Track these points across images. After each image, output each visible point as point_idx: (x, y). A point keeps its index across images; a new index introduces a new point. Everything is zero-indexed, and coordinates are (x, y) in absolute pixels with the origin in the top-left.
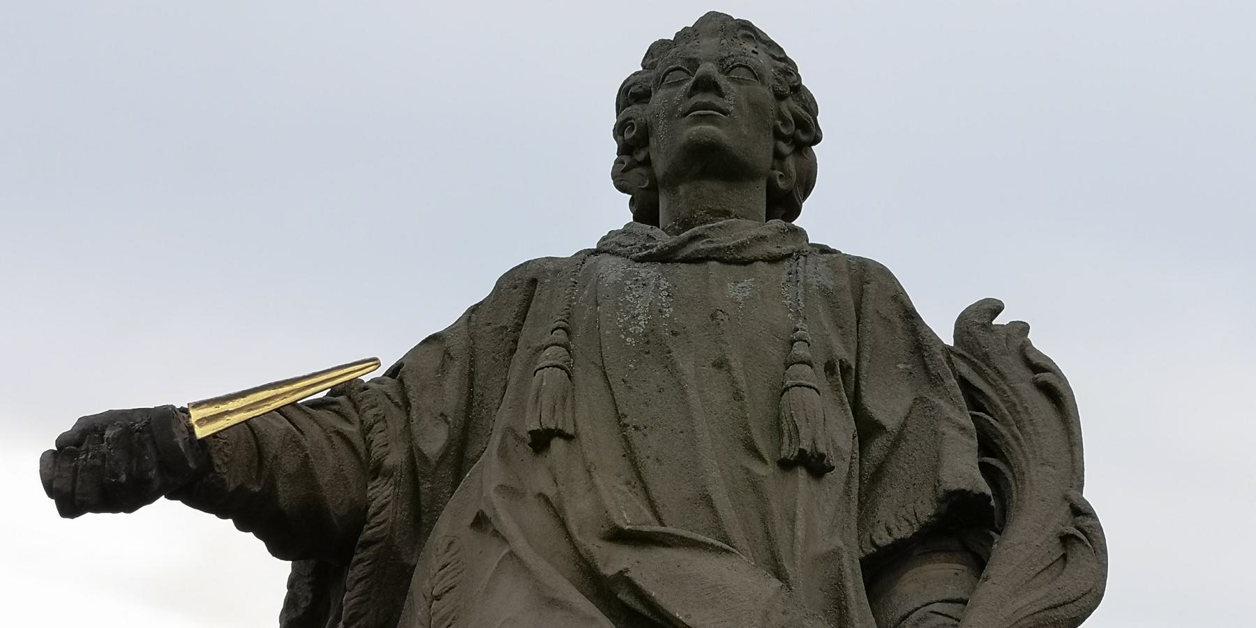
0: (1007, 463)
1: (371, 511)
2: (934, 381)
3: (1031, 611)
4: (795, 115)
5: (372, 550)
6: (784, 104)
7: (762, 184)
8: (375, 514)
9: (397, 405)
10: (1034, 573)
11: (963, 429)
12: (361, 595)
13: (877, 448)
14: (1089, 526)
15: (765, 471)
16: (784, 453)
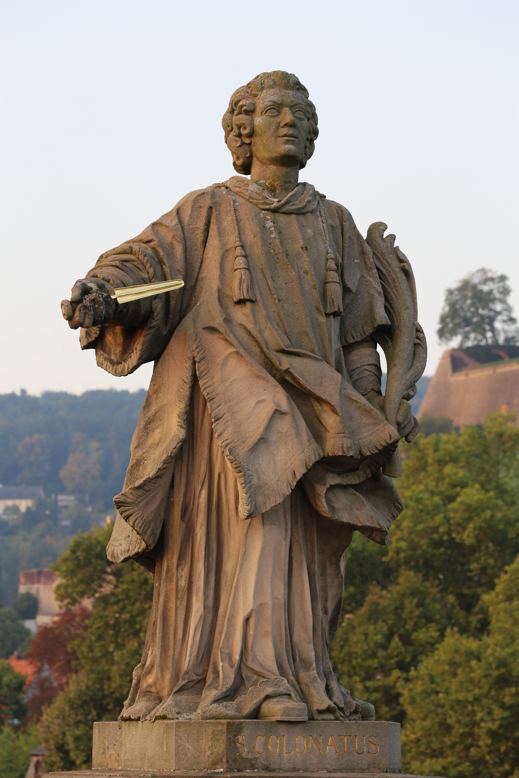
1: (156, 314)
2: (369, 270)
5: (153, 330)
9: (157, 262)
11: (379, 293)
14: (422, 337)
15: (322, 319)
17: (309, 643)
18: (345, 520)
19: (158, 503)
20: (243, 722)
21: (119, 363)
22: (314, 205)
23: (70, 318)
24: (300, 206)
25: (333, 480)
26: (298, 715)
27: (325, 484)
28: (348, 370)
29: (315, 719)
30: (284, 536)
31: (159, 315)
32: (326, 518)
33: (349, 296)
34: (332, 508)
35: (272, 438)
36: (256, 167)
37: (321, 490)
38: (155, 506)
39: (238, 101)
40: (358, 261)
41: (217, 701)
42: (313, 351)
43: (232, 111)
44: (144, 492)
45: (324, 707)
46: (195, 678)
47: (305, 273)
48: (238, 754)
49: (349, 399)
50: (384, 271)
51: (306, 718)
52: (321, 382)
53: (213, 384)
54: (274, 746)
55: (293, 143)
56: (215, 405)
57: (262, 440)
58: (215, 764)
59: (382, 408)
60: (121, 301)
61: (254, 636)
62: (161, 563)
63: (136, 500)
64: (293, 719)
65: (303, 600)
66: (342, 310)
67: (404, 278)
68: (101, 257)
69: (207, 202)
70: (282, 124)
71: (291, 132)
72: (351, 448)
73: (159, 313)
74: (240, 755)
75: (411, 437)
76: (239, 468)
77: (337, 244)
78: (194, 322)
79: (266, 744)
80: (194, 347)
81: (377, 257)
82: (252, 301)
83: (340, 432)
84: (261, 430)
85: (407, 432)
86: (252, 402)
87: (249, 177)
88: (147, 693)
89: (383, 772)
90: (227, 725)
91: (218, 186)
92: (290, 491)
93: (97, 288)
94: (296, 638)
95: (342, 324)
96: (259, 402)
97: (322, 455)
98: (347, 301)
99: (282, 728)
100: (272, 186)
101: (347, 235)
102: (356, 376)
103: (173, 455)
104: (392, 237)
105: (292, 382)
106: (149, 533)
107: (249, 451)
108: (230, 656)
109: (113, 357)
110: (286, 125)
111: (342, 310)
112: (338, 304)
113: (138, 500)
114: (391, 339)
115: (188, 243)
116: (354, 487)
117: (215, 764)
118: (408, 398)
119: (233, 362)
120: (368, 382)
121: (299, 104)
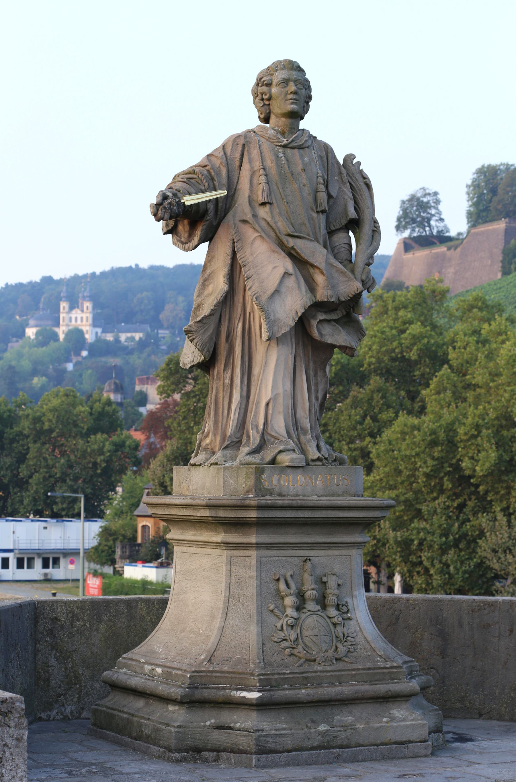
5: (208, 222)
11: (351, 198)
15: (315, 215)
17: (306, 418)
18: (329, 342)
21: (186, 243)
22: (309, 143)
23: (155, 215)
24: (301, 143)
25: (322, 316)
26: (299, 463)
27: (316, 319)
28: (331, 247)
32: (317, 340)
33: (332, 201)
34: (321, 334)
35: (283, 290)
36: (273, 119)
37: (314, 323)
38: (209, 333)
39: (262, 78)
41: (249, 454)
42: (309, 235)
43: (257, 84)
45: (315, 457)
46: (235, 440)
49: (332, 265)
50: (354, 184)
51: (305, 464)
54: (284, 481)
56: (247, 269)
57: (277, 291)
58: (248, 492)
59: (353, 271)
60: (187, 204)
61: (272, 414)
62: (214, 369)
64: (296, 464)
65: (302, 391)
66: (327, 209)
67: (366, 189)
68: (175, 176)
69: (242, 141)
70: (289, 92)
75: (370, 289)
76: (262, 309)
77: (324, 167)
78: (234, 216)
79: (279, 480)
80: (234, 232)
81: (349, 176)
84: (276, 285)
85: (368, 286)
86: (270, 267)
87: (268, 125)
88: (206, 449)
91: (249, 131)
94: (298, 415)
95: (327, 218)
96: (274, 267)
97: (314, 301)
98: (331, 204)
99: (289, 470)
100: (283, 131)
101: (330, 162)
102: (336, 251)
104: (359, 163)
105: (296, 255)
106: (205, 350)
108: (257, 427)
109: (183, 239)
110: (291, 93)
111: (327, 209)
112: (325, 205)
114: (358, 227)
115: (230, 167)
116: (335, 321)
117: (248, 492)
118: (369, 264)
119: (258, 242)
120: (344, 255)
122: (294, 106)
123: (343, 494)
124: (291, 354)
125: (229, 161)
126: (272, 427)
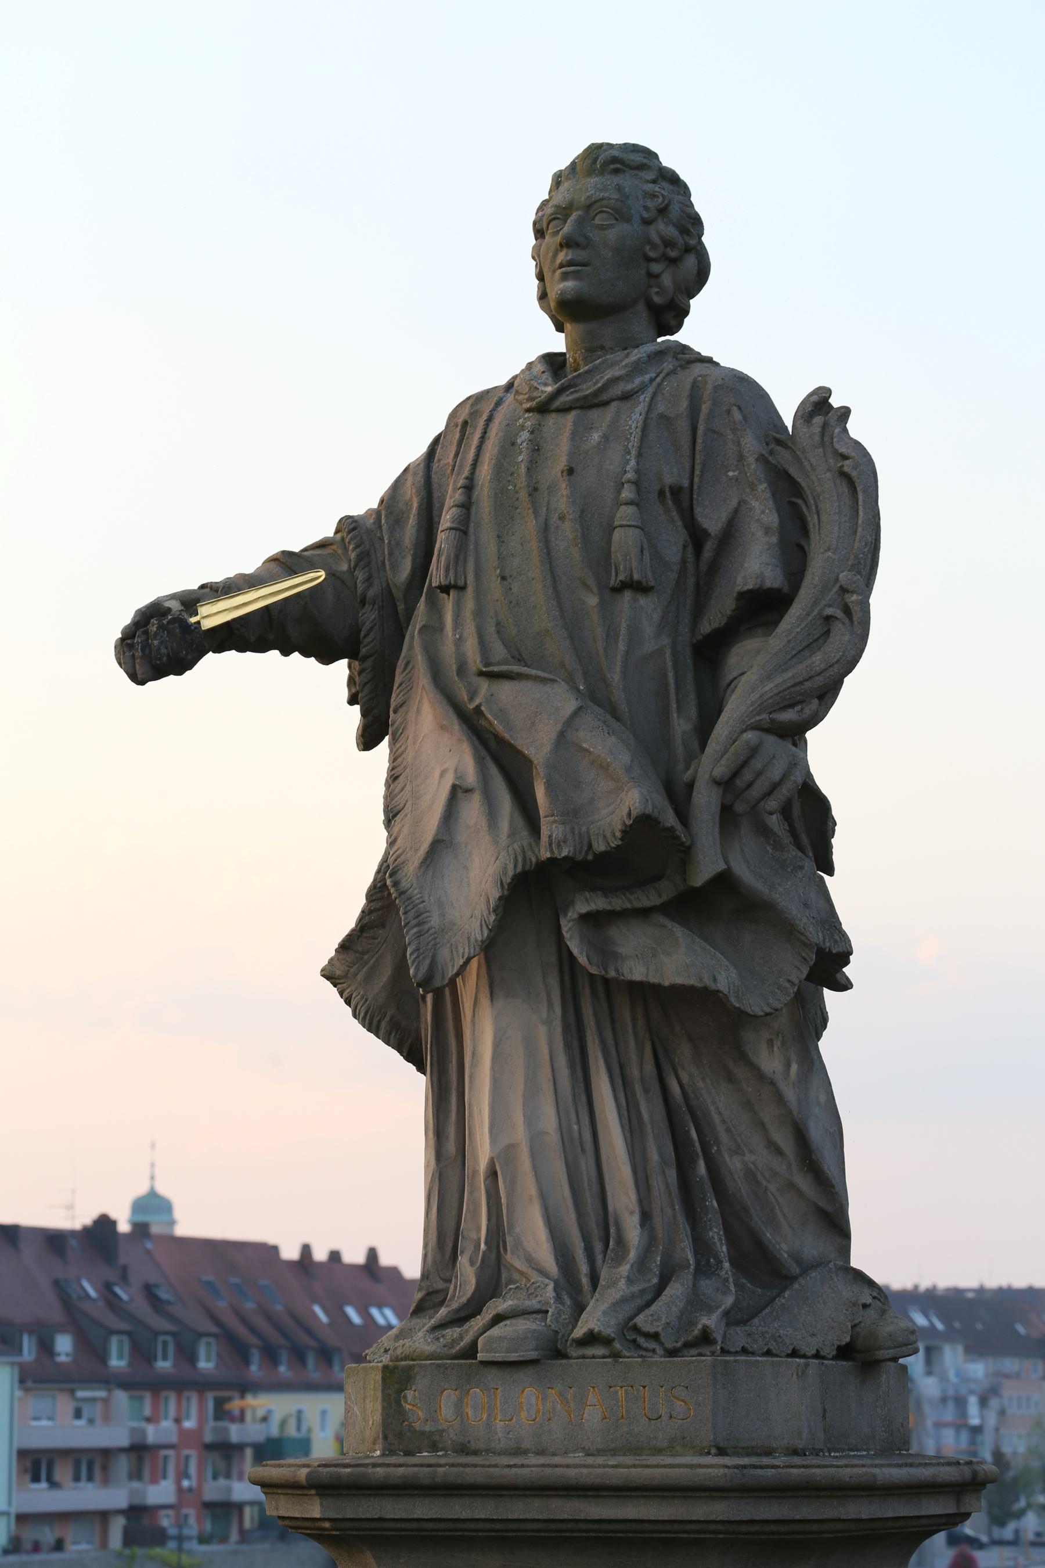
0: (809, 545)
1: (362, 634)
3: (777, 691)
4: (662, 238)
6: (652, 227)
7: (641, 306)
8: (365, 637)
10: (789, 657)
11: (767, 531)
12: (370, 694)
13: (708, 550)
16: (612, 583)
17: (632, 1213)
19: (389, 973)
20: (414, 1365)
26: (508, 1350)
29: (570, 1355)
30: (545, 1016)
31: (372, 635)
35: (462, 836)
38: (385, 979)
40: (736, 473)
44: (357, 955)
47: (560, 518)
48: (406, 1423)
52: (533, 723)
53: (406, 748)
55: (576, 275)
60: (207, 624)
63: (349, 971)
71: (569, 257)
72: (564, 842)
73: (371, 629)
74: (410, 1426)
79: (459, 1406)
82: (456, 587)
83: (547, 814)
89: (701, 1455)
90: (382, 1372)
92: (486, 933)
93: (181, 608)
99: (492, 1376)
103: (379, 885)
107: (420, 867)
113: (352, 970)
121: (602, 199)
122: (570, 284)
123: (670, 1449)
124: (548, 1022)
125: (435, 478)
126: (518, 1244)
